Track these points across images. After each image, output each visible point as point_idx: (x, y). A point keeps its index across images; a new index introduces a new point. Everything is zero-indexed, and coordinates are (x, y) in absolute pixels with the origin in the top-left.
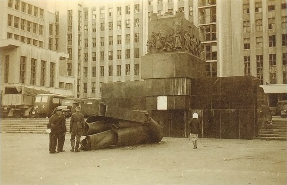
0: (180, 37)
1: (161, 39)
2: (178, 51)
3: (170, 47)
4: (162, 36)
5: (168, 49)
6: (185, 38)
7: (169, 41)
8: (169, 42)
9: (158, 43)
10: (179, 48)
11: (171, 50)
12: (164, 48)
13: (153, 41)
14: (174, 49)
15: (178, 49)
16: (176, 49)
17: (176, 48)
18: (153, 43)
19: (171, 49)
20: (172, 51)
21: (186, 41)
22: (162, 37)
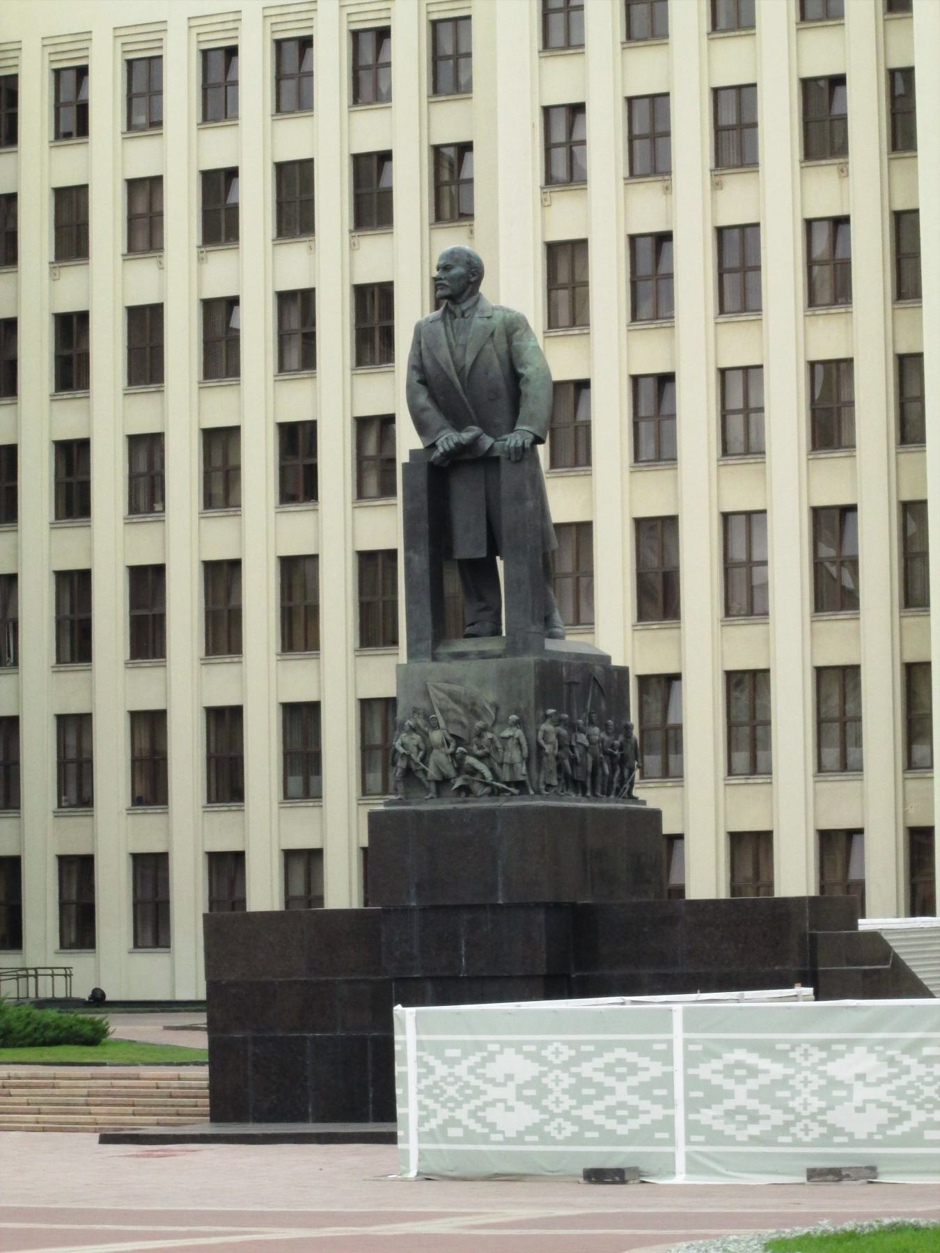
0: (523, 740)
1: (449, 745)
2: (513, 794)
3: (484, 777)
4: (451, 732)
5: (477, 788)
6: (542, 742)
7: (479, 752)
8: (480, 758)
9: (439, 757)
10: (521, 785)
11: (487, 789)
12: (458, 783)
13: (415, 749)
14: (497, 787)
15: (515, 791)
16: (504, 786)
17: (508, 784)
18: (418, 760)
19: (486, 785)
20: (492, 794)
21: (547, 755)
22: (452, 736)
